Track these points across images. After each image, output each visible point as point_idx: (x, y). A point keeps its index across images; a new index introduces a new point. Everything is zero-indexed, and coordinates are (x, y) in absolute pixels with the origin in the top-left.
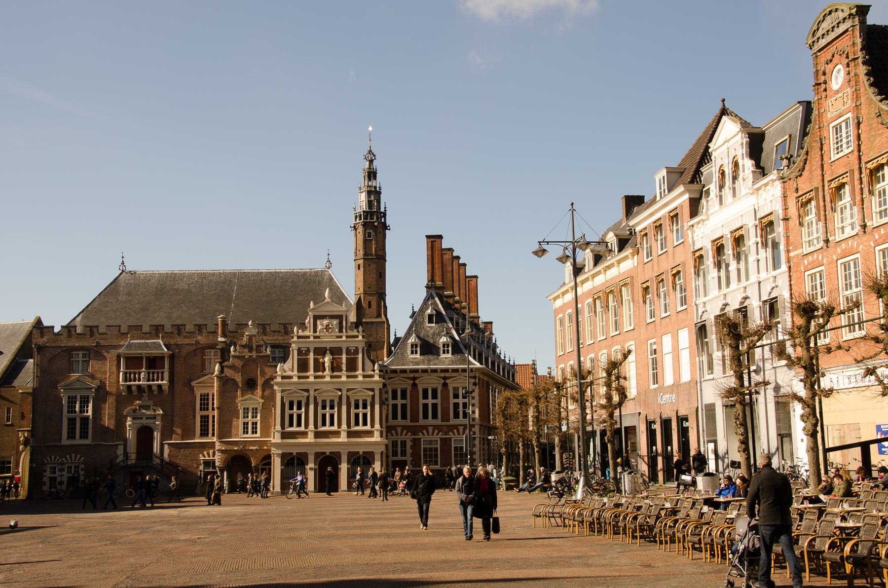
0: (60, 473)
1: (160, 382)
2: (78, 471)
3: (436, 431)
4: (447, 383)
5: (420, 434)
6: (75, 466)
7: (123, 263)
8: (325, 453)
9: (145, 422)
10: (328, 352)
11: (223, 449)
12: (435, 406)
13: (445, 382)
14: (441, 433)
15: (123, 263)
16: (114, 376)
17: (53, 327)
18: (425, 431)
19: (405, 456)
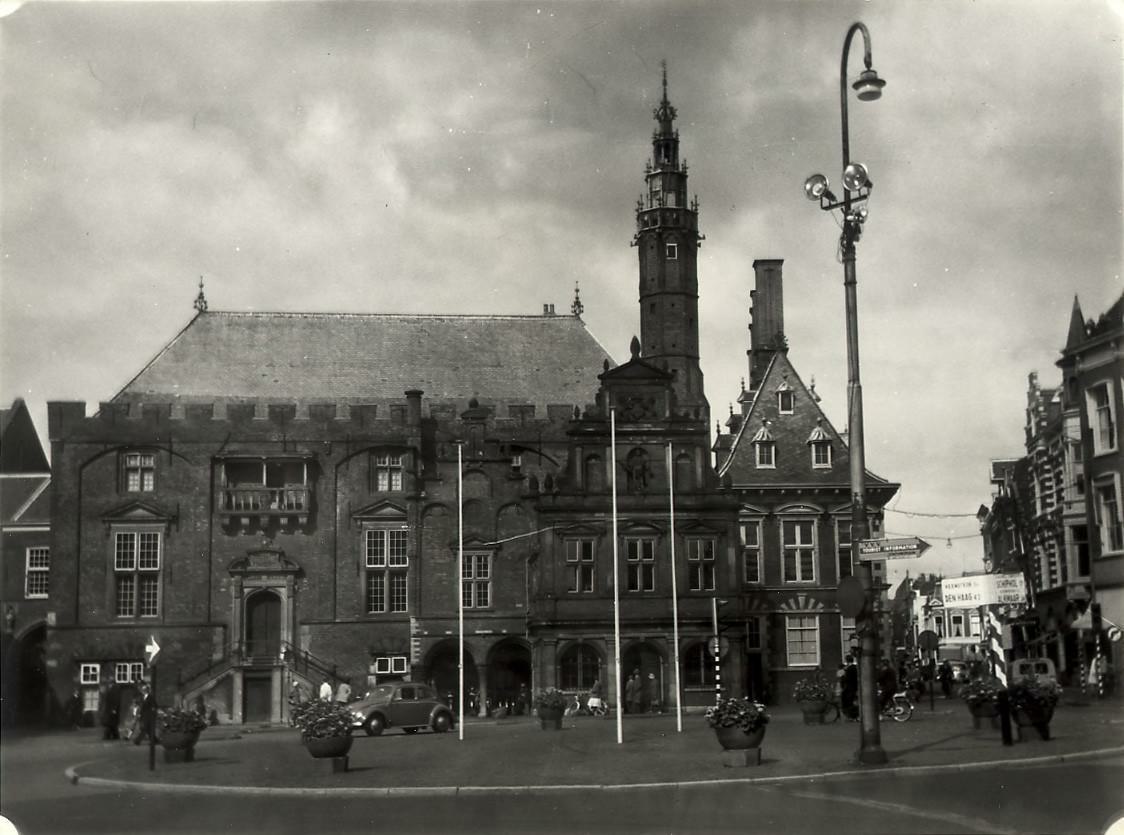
0: (104, 679)
1: (294, 511)
2: (139, 675)
3: (812, 601)
4: (830, 515)
5: (783, 606)
6: (133, 667)
7: (201, 296)
8: (638, 638)
9: (264, 582)
10: (638, 452)
11: (426, 633)
12: (806, 554)
13: (826, 513)
14: (821, 605)
15: (201, 296)
16: (204, 499)
17: (81, 406)
18: (791, 601)
19: (758, 646)
